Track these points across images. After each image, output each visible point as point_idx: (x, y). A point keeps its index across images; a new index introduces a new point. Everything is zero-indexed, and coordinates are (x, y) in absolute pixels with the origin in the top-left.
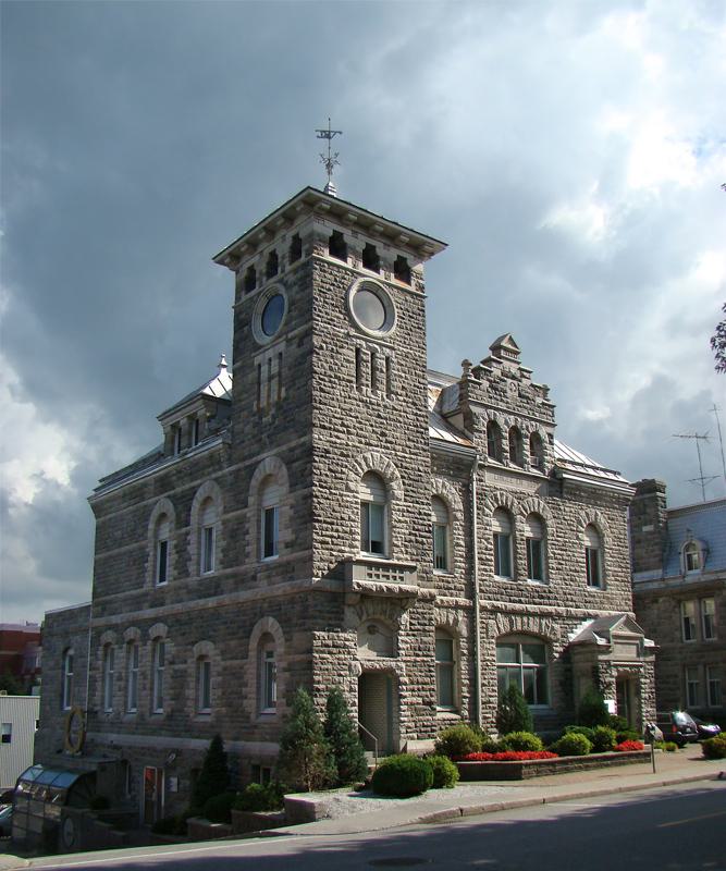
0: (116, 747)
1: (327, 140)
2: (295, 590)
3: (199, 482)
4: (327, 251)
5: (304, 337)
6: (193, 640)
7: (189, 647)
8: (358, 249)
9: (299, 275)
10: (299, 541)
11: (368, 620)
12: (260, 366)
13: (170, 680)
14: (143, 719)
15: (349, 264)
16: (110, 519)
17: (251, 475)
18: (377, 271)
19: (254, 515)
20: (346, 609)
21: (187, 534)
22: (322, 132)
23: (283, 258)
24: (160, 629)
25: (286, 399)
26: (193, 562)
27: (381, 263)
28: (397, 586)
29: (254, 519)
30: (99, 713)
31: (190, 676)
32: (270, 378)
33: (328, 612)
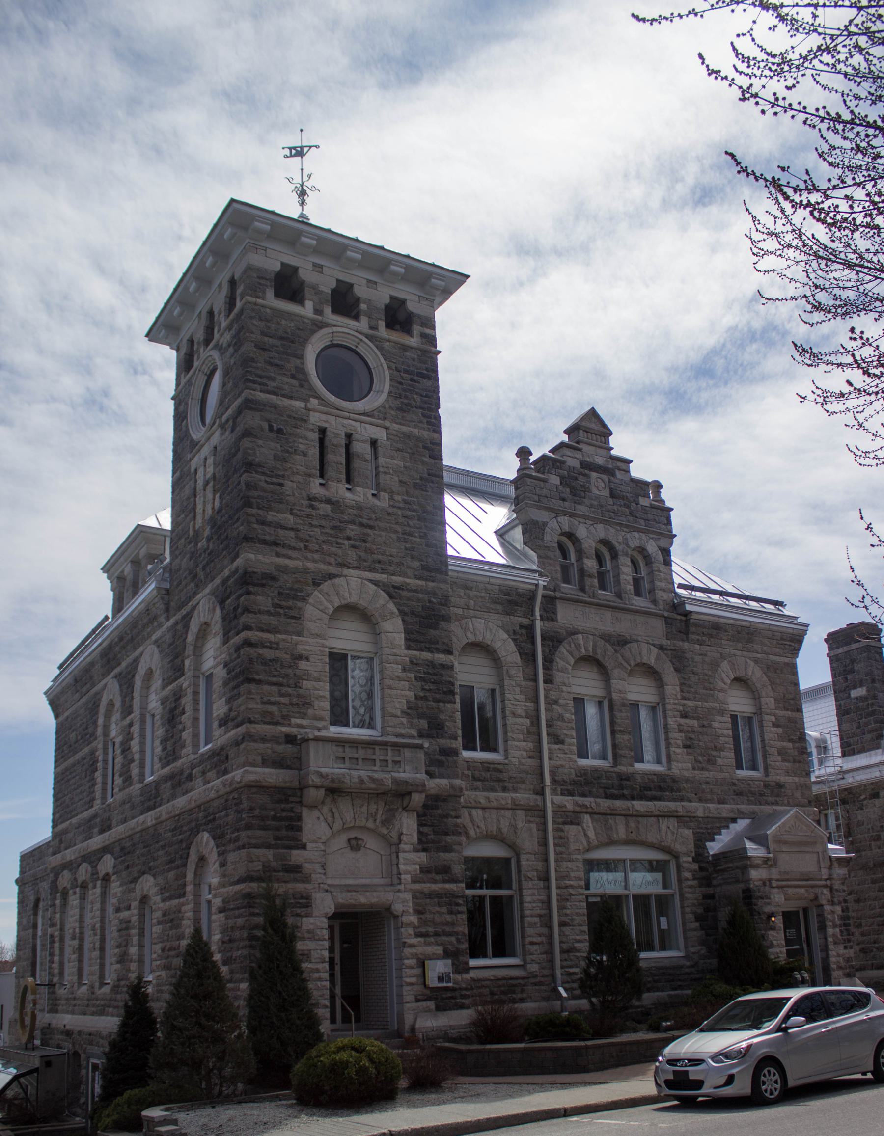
0: (68, 1033)
1: (298, 159)
2: (228, 789)
3: (141, 649)
4: (270, 293)
5: (236, 418)
6: (136, 875)
7: (132, 885)
8: (322, 288)
9: (233, 332)
10: (233, 714)
11: (345, 829)
12: (196, 470)
13: (116, 934)
14: (93, 993)
15: (307, 310)
16: (67, 717)
17: (187, 627)
18: (356, 317)
19: (189, 686)
20: (305, 812)
21: (131, 725)
22: (290, 149)
23: (220, 313)
24: (107, 864)
25: (220, 511)
26: (137, 763)
27: (363, 307)
28: (388, 776)
29: (189, 691)
30: (57, 986)
31: (134, 928)
32: (206, 483)
33: (274, 818)
